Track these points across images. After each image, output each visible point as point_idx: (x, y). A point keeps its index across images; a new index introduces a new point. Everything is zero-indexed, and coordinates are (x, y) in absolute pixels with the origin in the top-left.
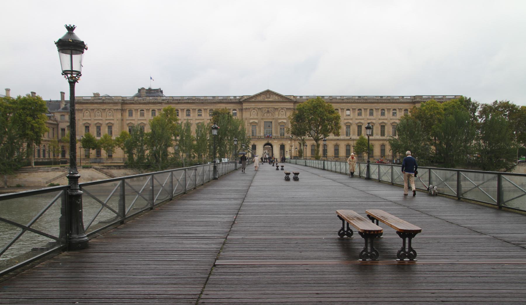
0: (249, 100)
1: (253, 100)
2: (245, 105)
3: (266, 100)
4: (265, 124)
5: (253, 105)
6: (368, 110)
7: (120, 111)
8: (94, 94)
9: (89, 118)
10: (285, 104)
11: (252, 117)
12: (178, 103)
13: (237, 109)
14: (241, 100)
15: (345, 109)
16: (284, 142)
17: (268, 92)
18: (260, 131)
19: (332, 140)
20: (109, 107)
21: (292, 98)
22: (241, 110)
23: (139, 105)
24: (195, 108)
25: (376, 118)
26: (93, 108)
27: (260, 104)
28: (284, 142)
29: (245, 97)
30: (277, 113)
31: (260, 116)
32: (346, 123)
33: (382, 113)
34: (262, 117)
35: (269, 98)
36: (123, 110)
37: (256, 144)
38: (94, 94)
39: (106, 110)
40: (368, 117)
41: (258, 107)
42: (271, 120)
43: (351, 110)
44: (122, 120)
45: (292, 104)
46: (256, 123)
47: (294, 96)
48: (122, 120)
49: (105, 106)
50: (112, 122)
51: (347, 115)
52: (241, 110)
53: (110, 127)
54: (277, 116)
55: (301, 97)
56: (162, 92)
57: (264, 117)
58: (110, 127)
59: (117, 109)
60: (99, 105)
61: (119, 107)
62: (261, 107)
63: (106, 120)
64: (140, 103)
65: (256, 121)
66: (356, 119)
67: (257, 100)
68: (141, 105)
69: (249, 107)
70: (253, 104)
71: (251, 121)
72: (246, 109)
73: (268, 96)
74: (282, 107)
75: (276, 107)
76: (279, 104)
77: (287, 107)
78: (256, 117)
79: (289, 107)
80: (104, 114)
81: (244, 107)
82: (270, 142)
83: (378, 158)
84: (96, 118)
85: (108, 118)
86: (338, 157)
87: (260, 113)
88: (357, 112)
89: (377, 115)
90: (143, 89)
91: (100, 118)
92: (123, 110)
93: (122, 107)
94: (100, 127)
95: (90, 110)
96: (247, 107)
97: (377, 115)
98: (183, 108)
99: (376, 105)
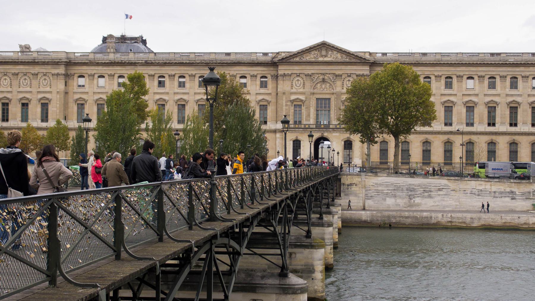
0: (289, 59)
1: (297, 59)
2: (282, 70)
3: (321, 59)
4: (317, 103)
5: (296, 69)
6: (508, 80)
7: (62, 77)
8: (21, 46)
9: (9, 89)
10: (355, 67)
11: (294, 90)
12: (165, 64)
13: (269, 76)
14: (276, 60)
15: (465, 77)
17: (324, 46)
18: (309, 115)
19: (439, 133)
20: (44, 71)
21: (367, 56)
22: (276, 77)
23: (96, 68)
24: (194, 73)
25: (502, 94)
26: (17, 72)
27: (308, 67)
29: (283, 55)
31: (308, 89)
32: (467, 102)
33: (262, 82)
34: (312, 91)
35: (326, 56)
36: (67, 76)
37: (300, 138)
38: (21, 46)
39: (39, 76)
40: (508, 91)
42: (327, 96)
43: (476, 78)
44: (66, 93)
45: (367, 68)
46: (301, 101)
47: (370, 54)
48: (66, 93)
49: (36, 69)
50: (48, 96)
51: (80, 86)
52: (276, 77)
53: (45, 106)
55: (384, 54)
56: (144, 42)
57: (315, 91)
58: (45, 106)
59: (58, 75)
60: (27, 67)
61: (61, 70)
63: (39, 92)
64: (98, 64)
65: (302, 97)
66: (485, 95)
67: (304, 60)
68: (100, 68)
69: (290, 72)
70: (296, 68)
71: (293, 97)
72: (284, 75)
73: (324, 53)
75: (337, 73)
76: (343, 67)
78: (301, 90)
79: (361, 73)
80: (35, 82)
81: (280, 72)
82: (326, 135)
83: (414, 166)
84: (21, 89)
85: (42, 89)
86: (451, 164)
87: (308, 84)
88: (486, 82)
89: (503, 88)
90: (111, 36)
91: (28, 89)
92: (67, 76)
93: (66, 70)
94: (7, 104)
95: (10, 75)
96: (286, 72)
97: (503, 88)
98: (173, 73)
99: (522, 69)
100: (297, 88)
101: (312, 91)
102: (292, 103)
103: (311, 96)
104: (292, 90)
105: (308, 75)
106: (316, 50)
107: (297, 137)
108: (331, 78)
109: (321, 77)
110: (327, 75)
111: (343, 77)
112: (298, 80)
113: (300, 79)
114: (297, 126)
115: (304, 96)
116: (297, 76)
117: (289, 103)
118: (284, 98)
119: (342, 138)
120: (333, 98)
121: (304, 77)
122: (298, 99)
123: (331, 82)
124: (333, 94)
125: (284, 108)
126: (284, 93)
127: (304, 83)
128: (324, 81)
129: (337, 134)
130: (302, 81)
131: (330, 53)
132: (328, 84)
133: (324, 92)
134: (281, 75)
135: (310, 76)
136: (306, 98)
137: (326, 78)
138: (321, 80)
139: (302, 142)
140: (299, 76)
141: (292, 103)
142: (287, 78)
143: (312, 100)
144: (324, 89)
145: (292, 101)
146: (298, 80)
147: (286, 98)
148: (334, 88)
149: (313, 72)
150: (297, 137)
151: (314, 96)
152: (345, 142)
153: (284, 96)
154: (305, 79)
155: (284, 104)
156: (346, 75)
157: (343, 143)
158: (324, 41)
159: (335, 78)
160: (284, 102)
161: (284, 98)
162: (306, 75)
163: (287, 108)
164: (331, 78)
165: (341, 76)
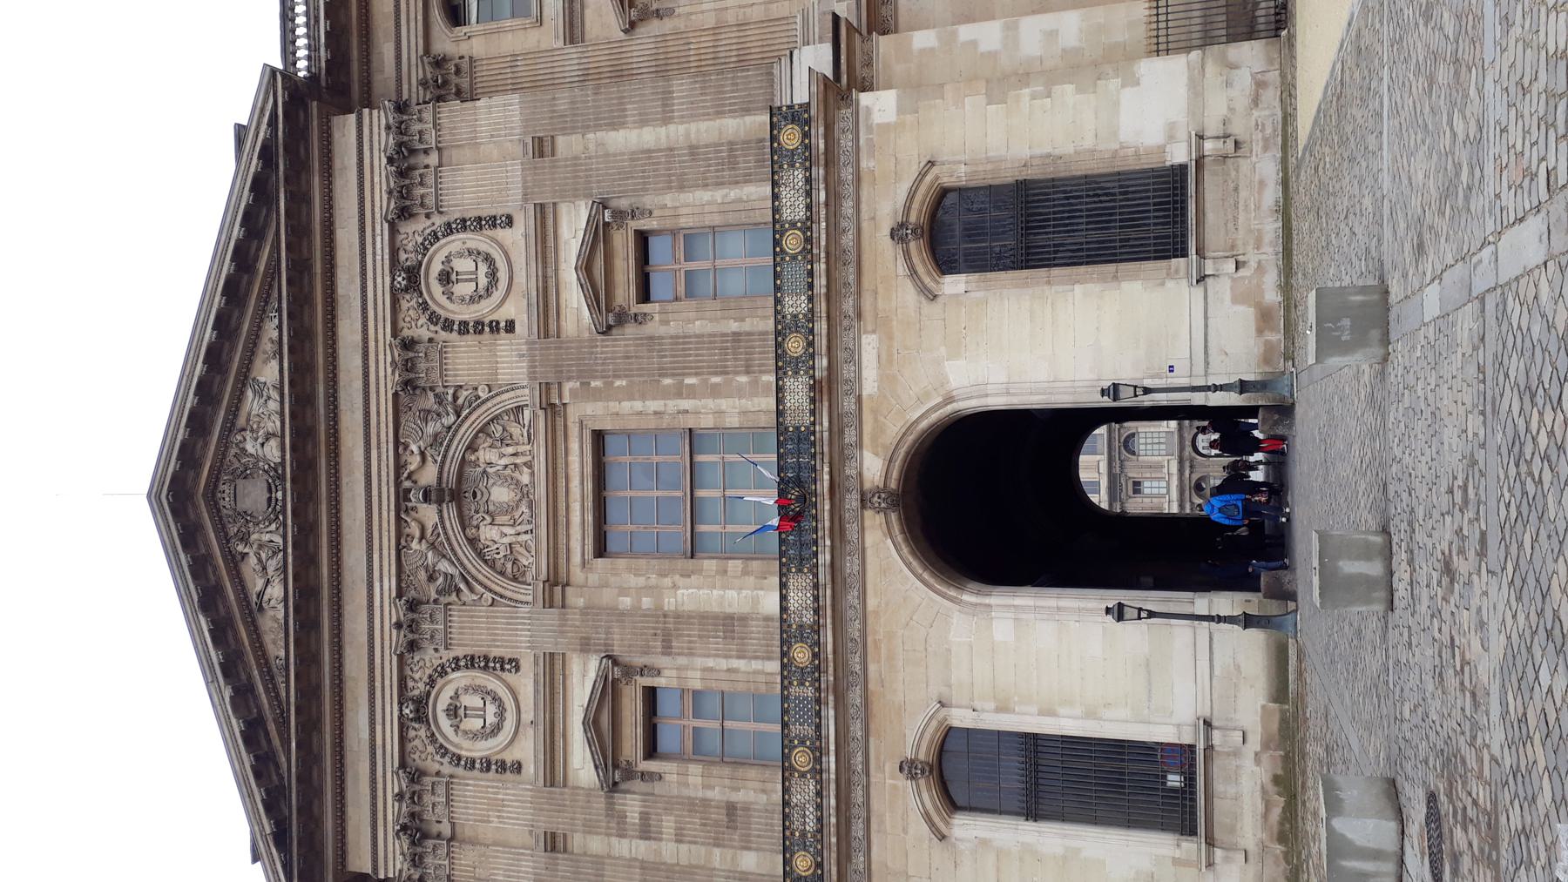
5: (368, 726)
11: (527, 750)
16: (886, 200)
18: (729, 626)
28: (886, 200)
30: (466, 362)
41: (389, 639)
54: (507, 365)
62: (389, 613)
69: (392, 784)
71: (581, 764)
73: (254, 496)
74: (381, 283)
75: (386, 379)
77: (381, 202)
78: (526, 683)
79: (380, 177)
87: (473, 626)
96: (392, 811)
100: (509, 725)
101: (524, 593)
102: (629, 774)
103: (576, 599)
104: (529, 769)
105: (413, 626)
106: (235, 562)
107: (909, 768)
108: (431, 428)
109: (429, 514)
110: (414, 462)
111: (422, 331)
112: (453, 711)
113: (443, 702)
114: (801, 759)
115: (575, 664)
116: (421, 716)
117: (632, 805)
118: (596, 844)
119: (907, 294)
120: (586, 412)
121: (429, 658)
122: (592, 723)
123: (466, 432)
124: (553, 410)
125: (669, 851)
126: (553, 843)
127: (471, 662)
128: (455, 493)
129: (869, 346)
130: (459, 679)
131: (250, 448)
132: (485, 455)
133: (541, 491)
134: (416, 860)
135: (413, 606)
136: (585, 647)
137: (429, 476)
138: (451, 511)
139: (961, 718)
140: (421, 704)
141: (629, 774)
142: (433, 802)
143: (606, 597)
144: (524, 493)
145: (615, 772)
146: (453, 711)
147: (590, 828)
148: (508, 400)
149: (390, 584)
150: (909, 768)
151: (577, 574)
152: (945, 264)
153: (577, 841)
154: (447, 655)
155: (641, 849)
156: (408, 303)
157: (954, 284)
158: (154, 496)
159: (430, 402)
160: (627, 848)
161: (596, 844)
162: (413, 646)
163: (668, 824)
164: (431, 428)
165: (408, 345)
